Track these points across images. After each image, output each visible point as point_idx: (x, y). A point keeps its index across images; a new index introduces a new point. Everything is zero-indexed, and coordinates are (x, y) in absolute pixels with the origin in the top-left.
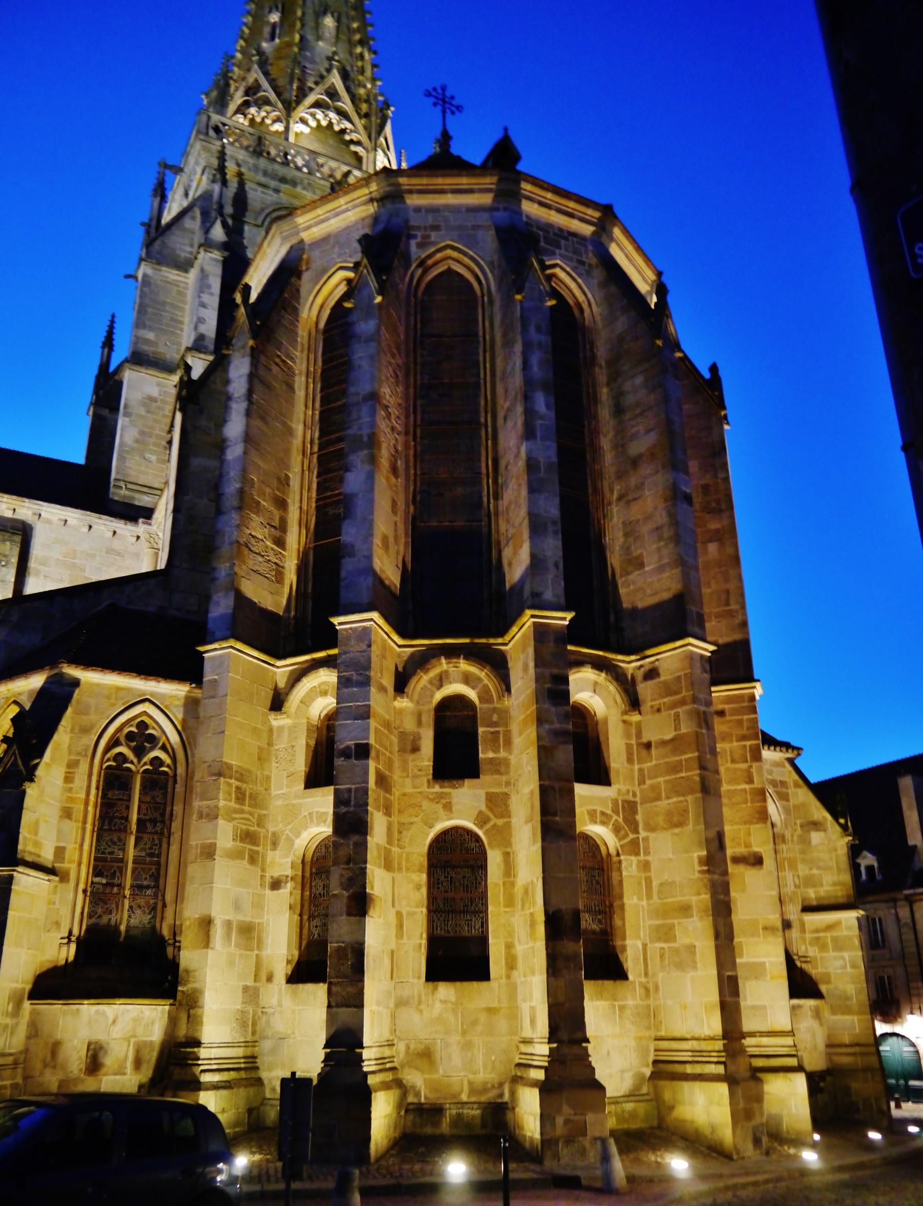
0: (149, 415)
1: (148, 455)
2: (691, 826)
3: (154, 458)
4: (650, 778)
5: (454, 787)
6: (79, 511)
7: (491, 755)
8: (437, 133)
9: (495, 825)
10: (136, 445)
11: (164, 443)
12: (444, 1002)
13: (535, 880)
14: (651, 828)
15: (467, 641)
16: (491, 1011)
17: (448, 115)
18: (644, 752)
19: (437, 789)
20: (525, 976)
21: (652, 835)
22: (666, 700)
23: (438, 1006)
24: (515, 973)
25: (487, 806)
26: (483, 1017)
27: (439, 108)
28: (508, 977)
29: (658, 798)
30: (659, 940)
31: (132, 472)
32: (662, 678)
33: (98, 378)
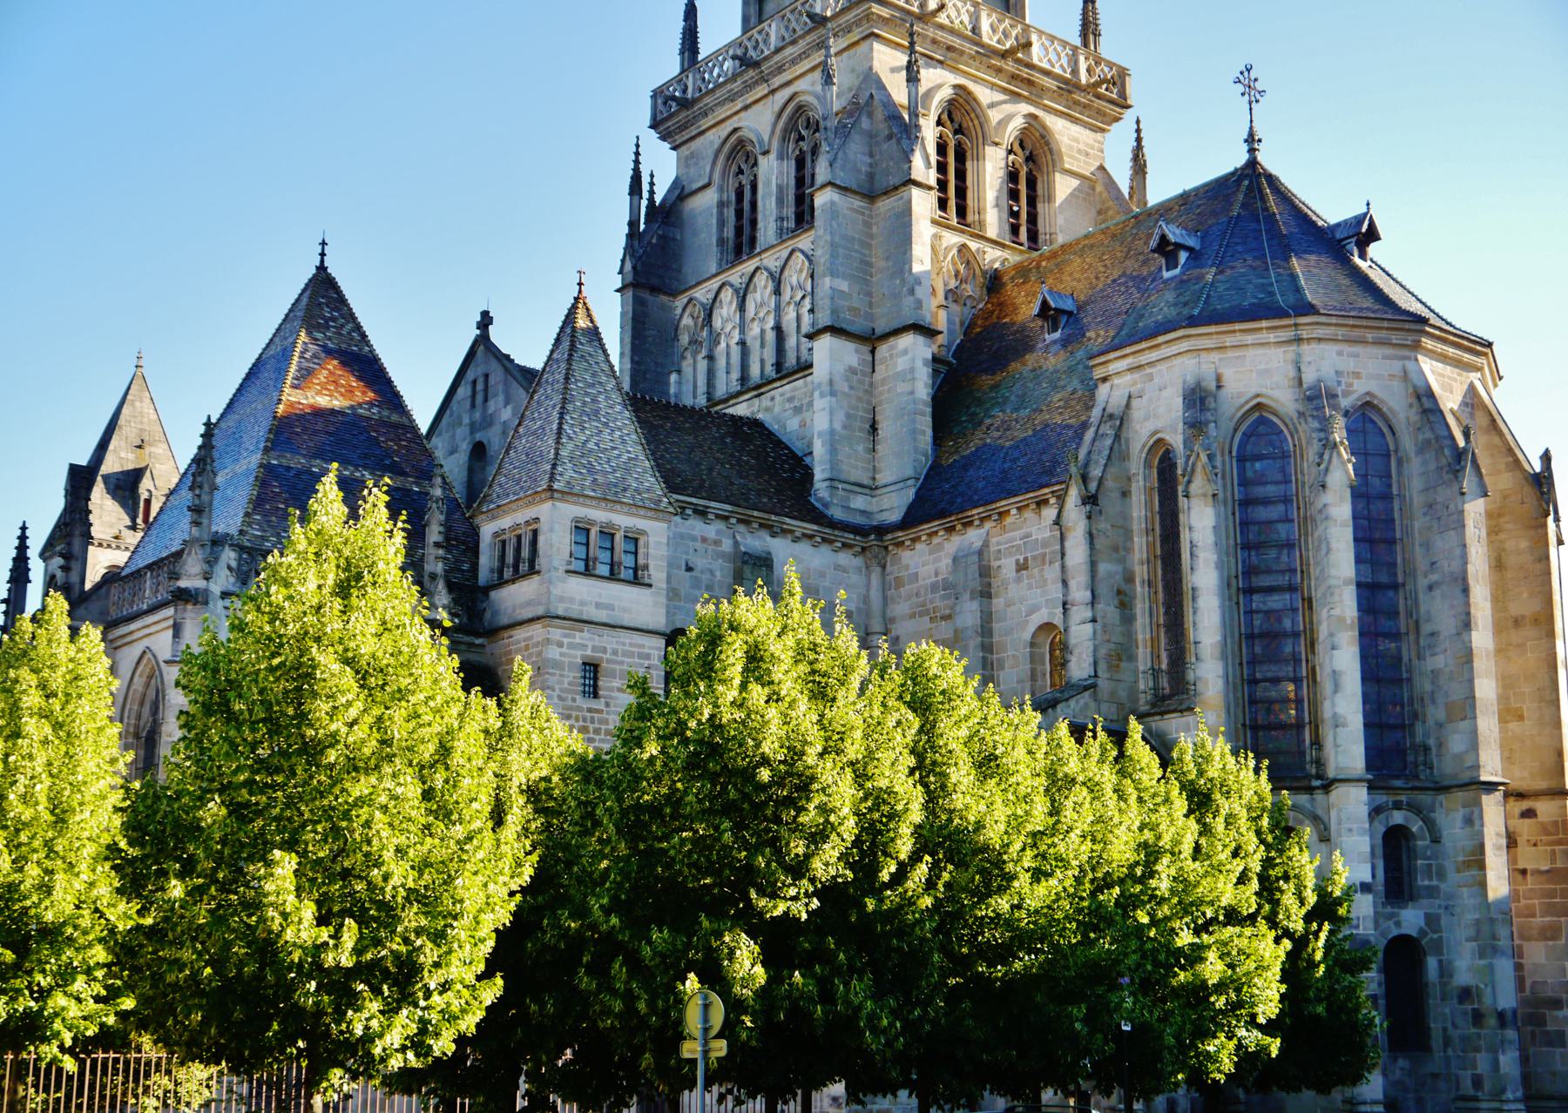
2: (1563, 941)
3: (860, 448)
4: (1525, 899)
7: (1426, 883)
10: (845, 432)
11: (867, 426)
12: (1402, 1069)
13: (1482, 986)
16: (1435, 1076)
17: (1254, 105)
18: (1520, 877)
19: (1389, 909)
20: (1464, 1051)
21: (1525, 944)
25: (1426, 924)
28: (1445, 1052)
29: (1533, 916)
31: (845, 467)
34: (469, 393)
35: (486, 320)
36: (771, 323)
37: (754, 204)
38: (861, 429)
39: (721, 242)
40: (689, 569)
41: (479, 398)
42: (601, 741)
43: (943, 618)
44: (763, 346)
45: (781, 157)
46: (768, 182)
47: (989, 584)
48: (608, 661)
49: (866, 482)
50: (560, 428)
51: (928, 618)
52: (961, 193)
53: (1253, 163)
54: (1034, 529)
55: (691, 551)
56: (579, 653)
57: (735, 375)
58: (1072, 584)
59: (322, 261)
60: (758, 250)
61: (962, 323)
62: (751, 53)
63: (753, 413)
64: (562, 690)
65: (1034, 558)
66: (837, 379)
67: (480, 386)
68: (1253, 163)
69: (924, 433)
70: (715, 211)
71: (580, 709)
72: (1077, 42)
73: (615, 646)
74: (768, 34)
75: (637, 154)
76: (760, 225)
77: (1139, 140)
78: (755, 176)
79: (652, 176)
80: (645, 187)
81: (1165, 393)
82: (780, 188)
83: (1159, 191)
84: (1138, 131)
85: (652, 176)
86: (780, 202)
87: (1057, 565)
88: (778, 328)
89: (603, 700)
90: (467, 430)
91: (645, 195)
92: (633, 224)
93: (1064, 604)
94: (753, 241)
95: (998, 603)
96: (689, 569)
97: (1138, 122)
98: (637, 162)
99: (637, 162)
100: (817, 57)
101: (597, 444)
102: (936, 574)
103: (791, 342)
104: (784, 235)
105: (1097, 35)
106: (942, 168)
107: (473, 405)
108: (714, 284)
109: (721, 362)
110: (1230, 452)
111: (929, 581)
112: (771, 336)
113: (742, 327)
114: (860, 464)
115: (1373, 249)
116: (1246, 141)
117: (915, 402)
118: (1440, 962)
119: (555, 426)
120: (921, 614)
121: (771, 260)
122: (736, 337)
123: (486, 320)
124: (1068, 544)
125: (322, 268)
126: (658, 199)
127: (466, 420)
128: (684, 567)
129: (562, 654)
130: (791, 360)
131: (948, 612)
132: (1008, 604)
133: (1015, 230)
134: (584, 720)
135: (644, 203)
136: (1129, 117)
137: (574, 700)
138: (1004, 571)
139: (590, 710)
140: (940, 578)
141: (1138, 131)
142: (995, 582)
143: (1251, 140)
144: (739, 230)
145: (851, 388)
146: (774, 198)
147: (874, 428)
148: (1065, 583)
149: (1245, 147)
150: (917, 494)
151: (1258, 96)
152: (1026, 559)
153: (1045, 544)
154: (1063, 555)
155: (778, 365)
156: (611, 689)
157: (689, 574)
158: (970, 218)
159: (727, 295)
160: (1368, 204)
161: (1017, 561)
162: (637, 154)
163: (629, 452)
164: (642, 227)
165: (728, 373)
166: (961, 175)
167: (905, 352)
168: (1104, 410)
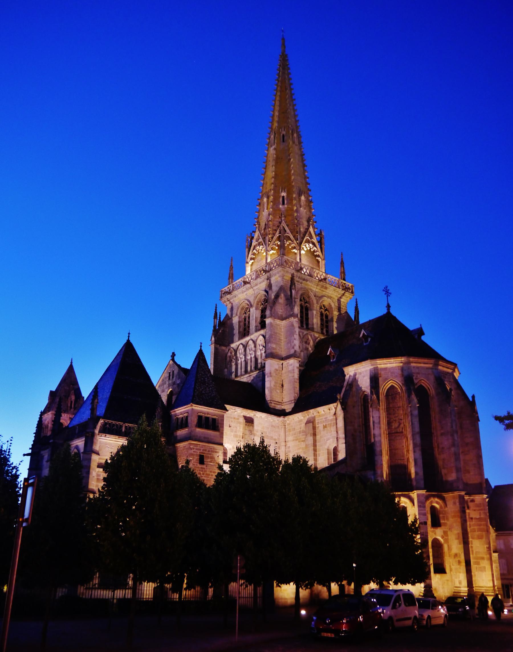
0: (276, 376)
1: (277, 391)
3: (279, 391)
5: (436, 529)
6: (266, 414)
7: (443, 521)
8: (386, 305)
9: (445, 538)
10: (274, 387)
11: (281, 386)
12: (438, 578)
13: (461, 553)
14: (473, 538)
15: (436, 493)
16: (448, 580)
17: (388, 297)
18: (471, 520)
19: (432, 529)
22: (477, 508)
23: (437, 579)
24: (452, 572)
26: (446, 582)
27: (386, 295)
28: (450, 573)
30: (475, 564)
31: (274, 397)
32: (476, 503)
33: (213, 331)
34: (168, 375)
35: (173, 355)
36: (253, 356)
37: (249, 322)
38: (279, 387)
40: (230, 427)
41: (171, 377)
42: (204, 477)
43: (302, 441)
44: (251, 361)
45: (256, 309)
46: (253, 316)
47: (316, 432)
48: (207, 454)
49: (280, 401)
50: (195, 388)
51: (298, 441)
52: (307, 319)
53: (389, 313)
54: (328, 416)
55: (231, 421)
56: (199, 451)
57: (243, 370)
58: (339, 432)
59: (129, 338)
61: (307, 356)
63: (248, 381)
64: (194, 462)
65: (328, 424)
66: (272, 372)
67: (171, 374)
68: (389, 313)
69: (297, 388)
70: (238, 324)
71: (198, 467)
73: (209, 449)
75: (216, 307)
76: (251, 328)
77: (357, 304)
78: (249, 314)
79: (220, 313)
80: (218, 316)
81: (365, 378)
82: (256, 317)
83: (363, 319)
85: (220, 313)
86: (256, 321)
87: (335, 426)
88: (255, 357)
89: (205, 465)
90: (168, 385)
91: (218, 318)
92: (215, 327)
93: (337, 438)
94: (249, 332)
95: (318, 437)
96: (230, 427)
98: (216, 310)
99: (216, 310)
101: (205, 392)
102: (300, 429)
103: (259, 361)
104: (257, 330)
106: (301, 312)
107: (169, 379)
108: (238, 343)
109: (239, 366)
110: (384, 395)
111: (298, 431)
112: (253, 359)
113: (245, 355)
114: (279, 396)
115: (423, 338)
116: (386, 307)
117: (294, 379)
118: (448, 545)
119: (193, 386)
120: (296, 440)
122: (243, 360)
123: (173, 355)
124: (338, 421)
125: (128, 341)
126: (222, 320)
127: (167, 383)
128: (228, 426)
129: (194, 452)
130: (259, 366)
131: (304, 439)
132: (321, 437)
133: (322, 329)
134: (200, 471)
135: (218, 321)
137: (197, 465)
138: (320, 428)
139: (201, 468)
140: (301, 429)
142: (317, 431)
143: (388, 306)
144: (245, 329)
145: (276, 375)
146: (254, 320)
147: (282, 386)
148: (337, 432)
149: (386, 309)
150: (295, 405)
151: (389, 294)
152: (326, 425)
153: (331, 420)
154: (336, 424)
156: (208, 462)
157: (230, 428)
158: (310, 326)
159: (241, 346)
160: (421, 325)
161: (324, 425)
162: (216, 307)
163: (214, 394)
164: (217, 327)
165: (241, 369)
166: (307, 315)
167: (291, 365)
168: (348, 382)
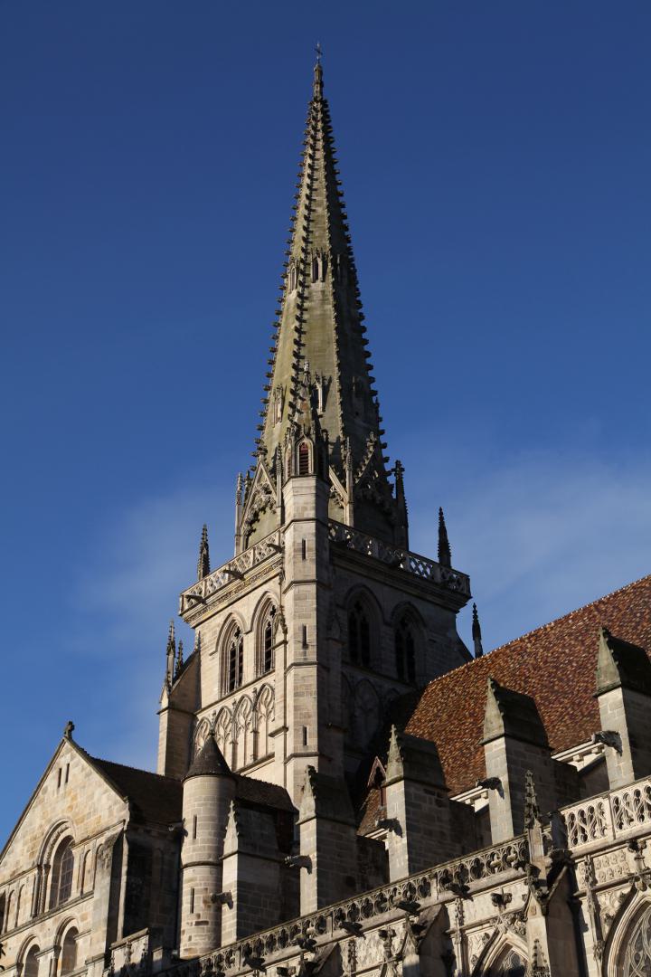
39: (222, 681)
60: (243, 684)
62: (240, 569)
72: (437, 560)
74: (249, 558)
79: (181, 644)
84: (475, 612)
85: (181, 644)
97: (475, 606)
100: (277, 570)
105: (449, 555)
121: (249, 692)
130: (262, 753)
133: (400, 671)
136: (470, 603)
141: (475, 612)
155: (255, 755)
